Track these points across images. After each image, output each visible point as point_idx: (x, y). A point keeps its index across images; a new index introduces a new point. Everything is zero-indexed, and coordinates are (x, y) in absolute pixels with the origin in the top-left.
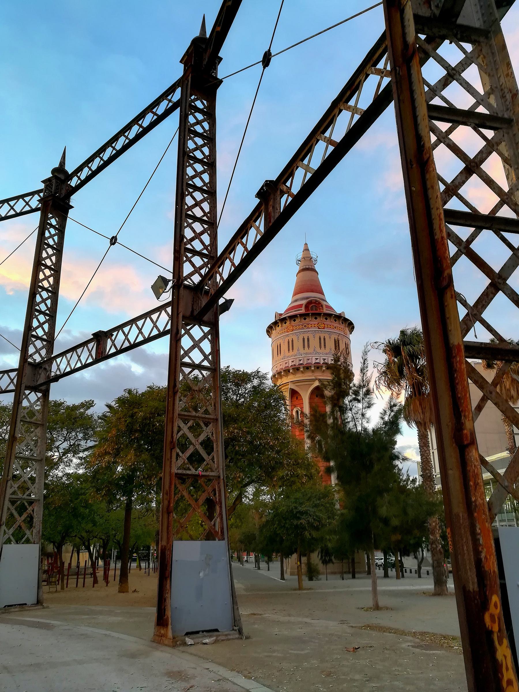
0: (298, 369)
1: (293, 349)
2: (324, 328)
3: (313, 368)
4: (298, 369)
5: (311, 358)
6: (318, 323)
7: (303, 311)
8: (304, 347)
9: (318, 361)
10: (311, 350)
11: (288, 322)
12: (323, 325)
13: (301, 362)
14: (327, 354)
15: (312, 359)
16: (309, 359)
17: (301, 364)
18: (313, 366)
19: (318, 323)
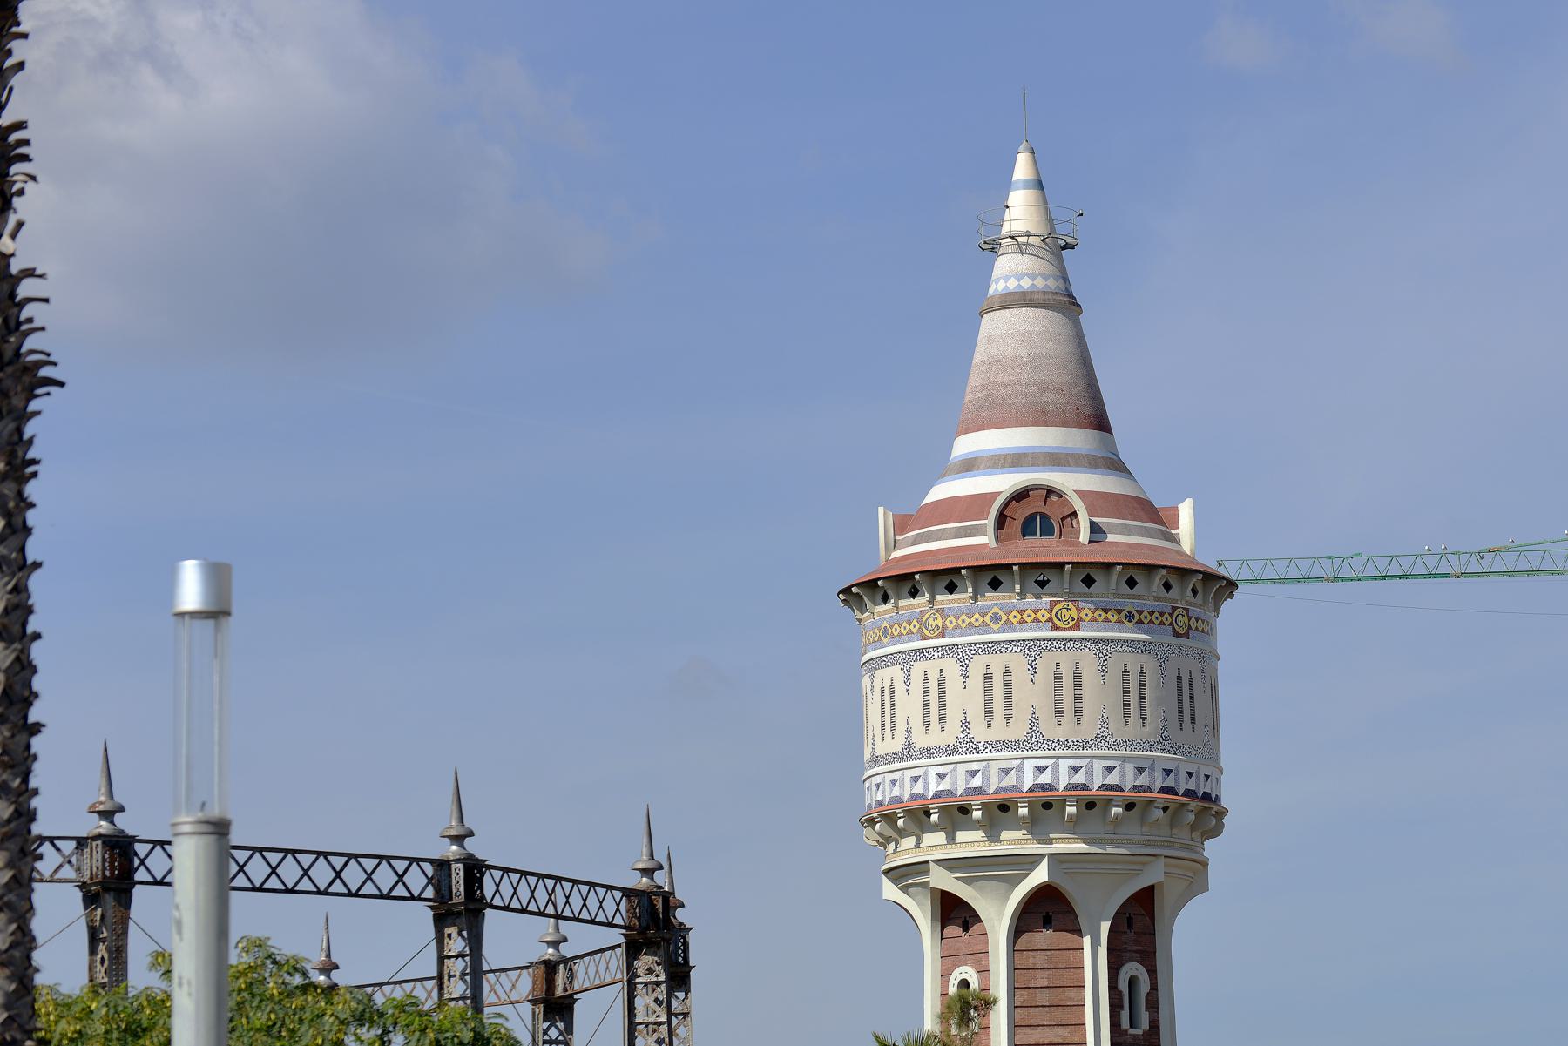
0: (965, 810)
2: (1076, 628)
4: (965, 810)
5: (1016, 763)
7: (982, 541)
9: (1045, 778)
12: (1074, 613)
13: (977, 782)
14: (1085, 744)
15: (1020, 769)
17: (977, 791)
18: (1022, 802)
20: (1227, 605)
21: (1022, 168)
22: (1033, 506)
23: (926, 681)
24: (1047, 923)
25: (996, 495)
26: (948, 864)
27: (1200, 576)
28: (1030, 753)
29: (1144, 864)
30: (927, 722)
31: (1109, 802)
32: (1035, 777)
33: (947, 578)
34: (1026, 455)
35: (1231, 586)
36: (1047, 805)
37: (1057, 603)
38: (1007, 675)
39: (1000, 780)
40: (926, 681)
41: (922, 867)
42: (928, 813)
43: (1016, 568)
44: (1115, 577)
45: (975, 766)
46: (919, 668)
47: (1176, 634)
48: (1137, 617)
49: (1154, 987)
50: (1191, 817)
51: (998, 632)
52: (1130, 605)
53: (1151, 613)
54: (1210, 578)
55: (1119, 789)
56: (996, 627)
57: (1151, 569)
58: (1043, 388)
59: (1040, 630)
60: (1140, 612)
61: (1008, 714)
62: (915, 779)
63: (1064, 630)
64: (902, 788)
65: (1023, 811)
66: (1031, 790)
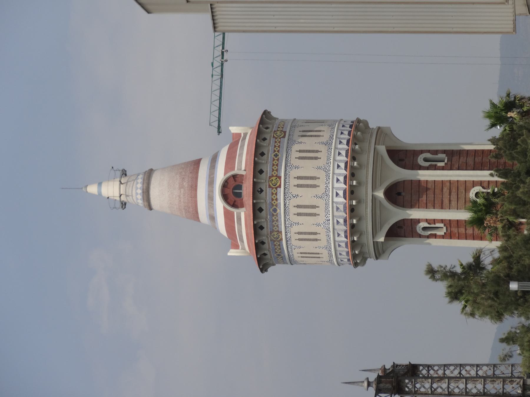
0: (353, 226)
1: (315, 234)
2: (280, 178)
3: (354, 203)
5: (335, 205)
6: (270, 187)
8: (315, 215)
9: (341, 193)
10: (320, 203)
11: (264, 238)
12: (274, 178)
14: (328, 176)
15: (337, 203)
16: (338, 209)
17: (345, 221)
19: (270, 187)
20: (274, 114)
21: (93, 189)
22: (229, 191)
23: (300, 240)
24: (399, 194)
25: (224, 208)
26: (374, 234)
27: (261, 126)
28: (331, 199)
29: (378, 153)
30: (316, 240)
31: (352, 167)
32: (340, 197)
33: (257, 229)
34: (209, 195)
35: (266, 114)
36: (352, 192)
37: (269, 185)
38: (298, 206)
39: (341, 211)
40: (300, 240)
41: (376, 244)
42: (353, 241)
43: (254, 201)
44: (260, 161)
45: (335, 221)
46: (294, 242)
47: (284, 137)
48: (276, 152)
49: (429, 151)
50: (359, 133)
51: (280, 209)
52: (271, 155)
53: (275, 146)
54: (262, 122)
55: (346, 163)
56: (278, 211)
57: (257, 146)
58: (181, 187)
59: (280, 192)
60: (275, 151)
61: (314, 207)
62: (339, 246)
63: (281, 182)
64: (342, 251)
65: (354, 203)
66: (345, 199)
